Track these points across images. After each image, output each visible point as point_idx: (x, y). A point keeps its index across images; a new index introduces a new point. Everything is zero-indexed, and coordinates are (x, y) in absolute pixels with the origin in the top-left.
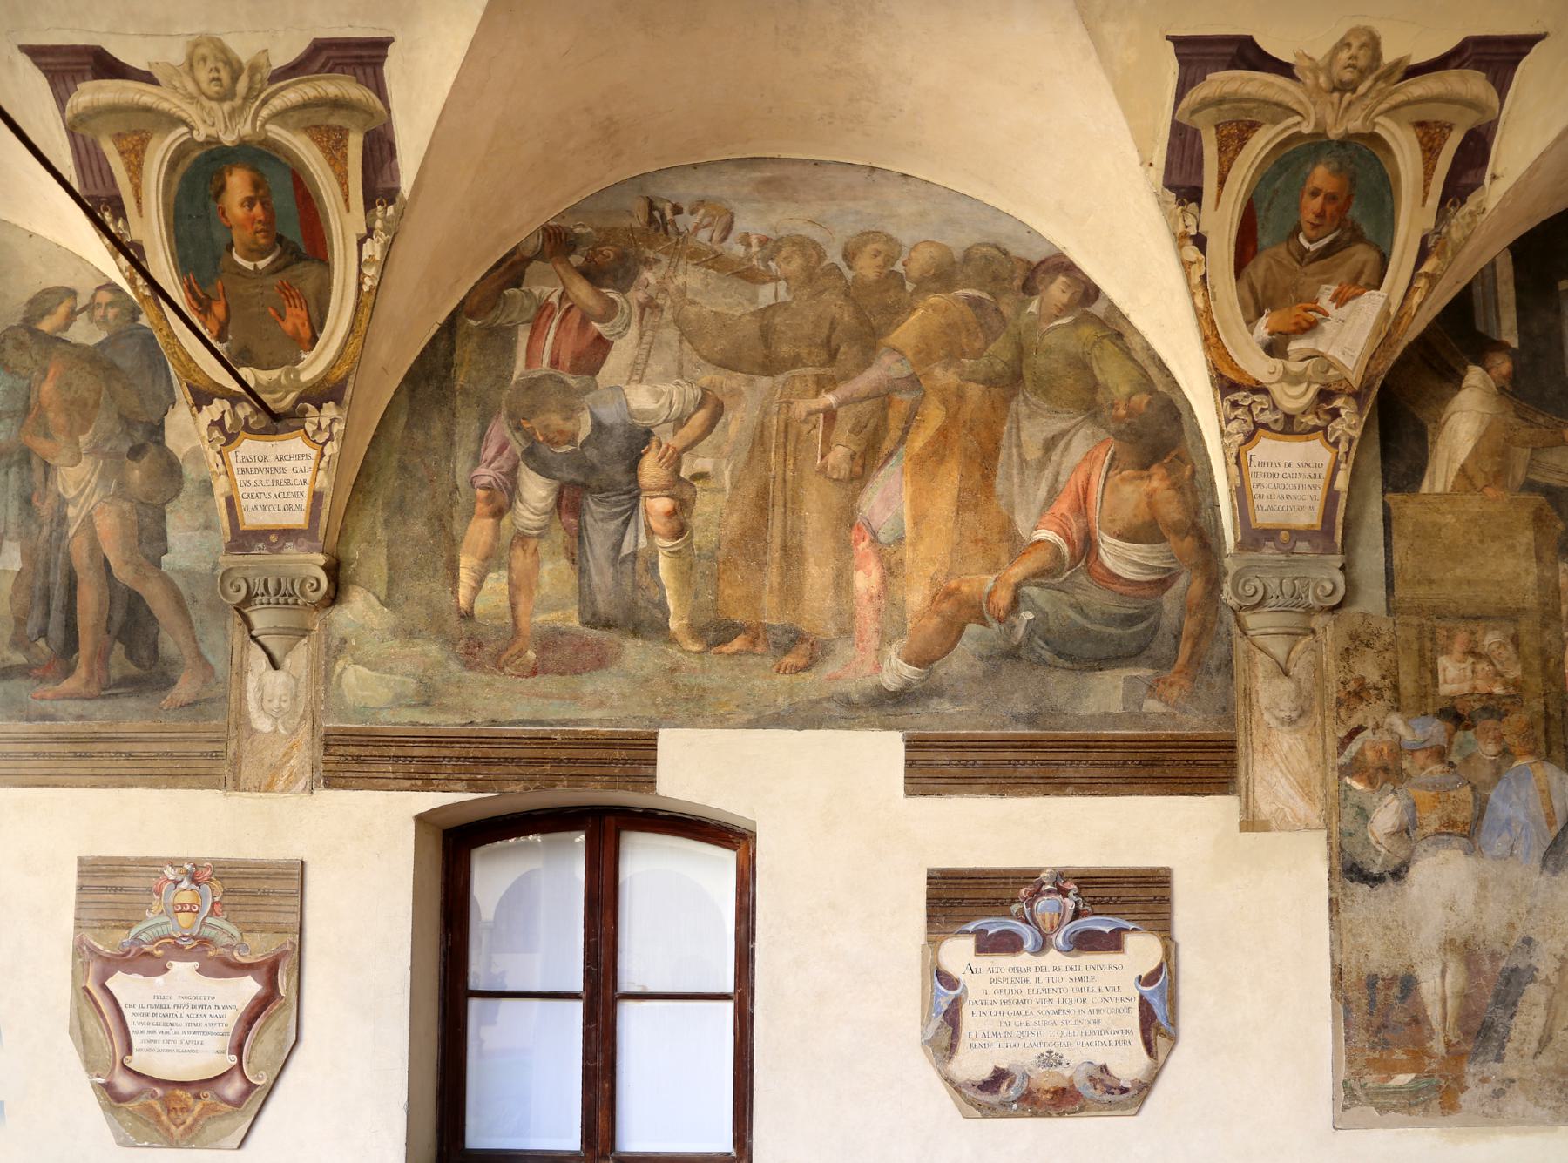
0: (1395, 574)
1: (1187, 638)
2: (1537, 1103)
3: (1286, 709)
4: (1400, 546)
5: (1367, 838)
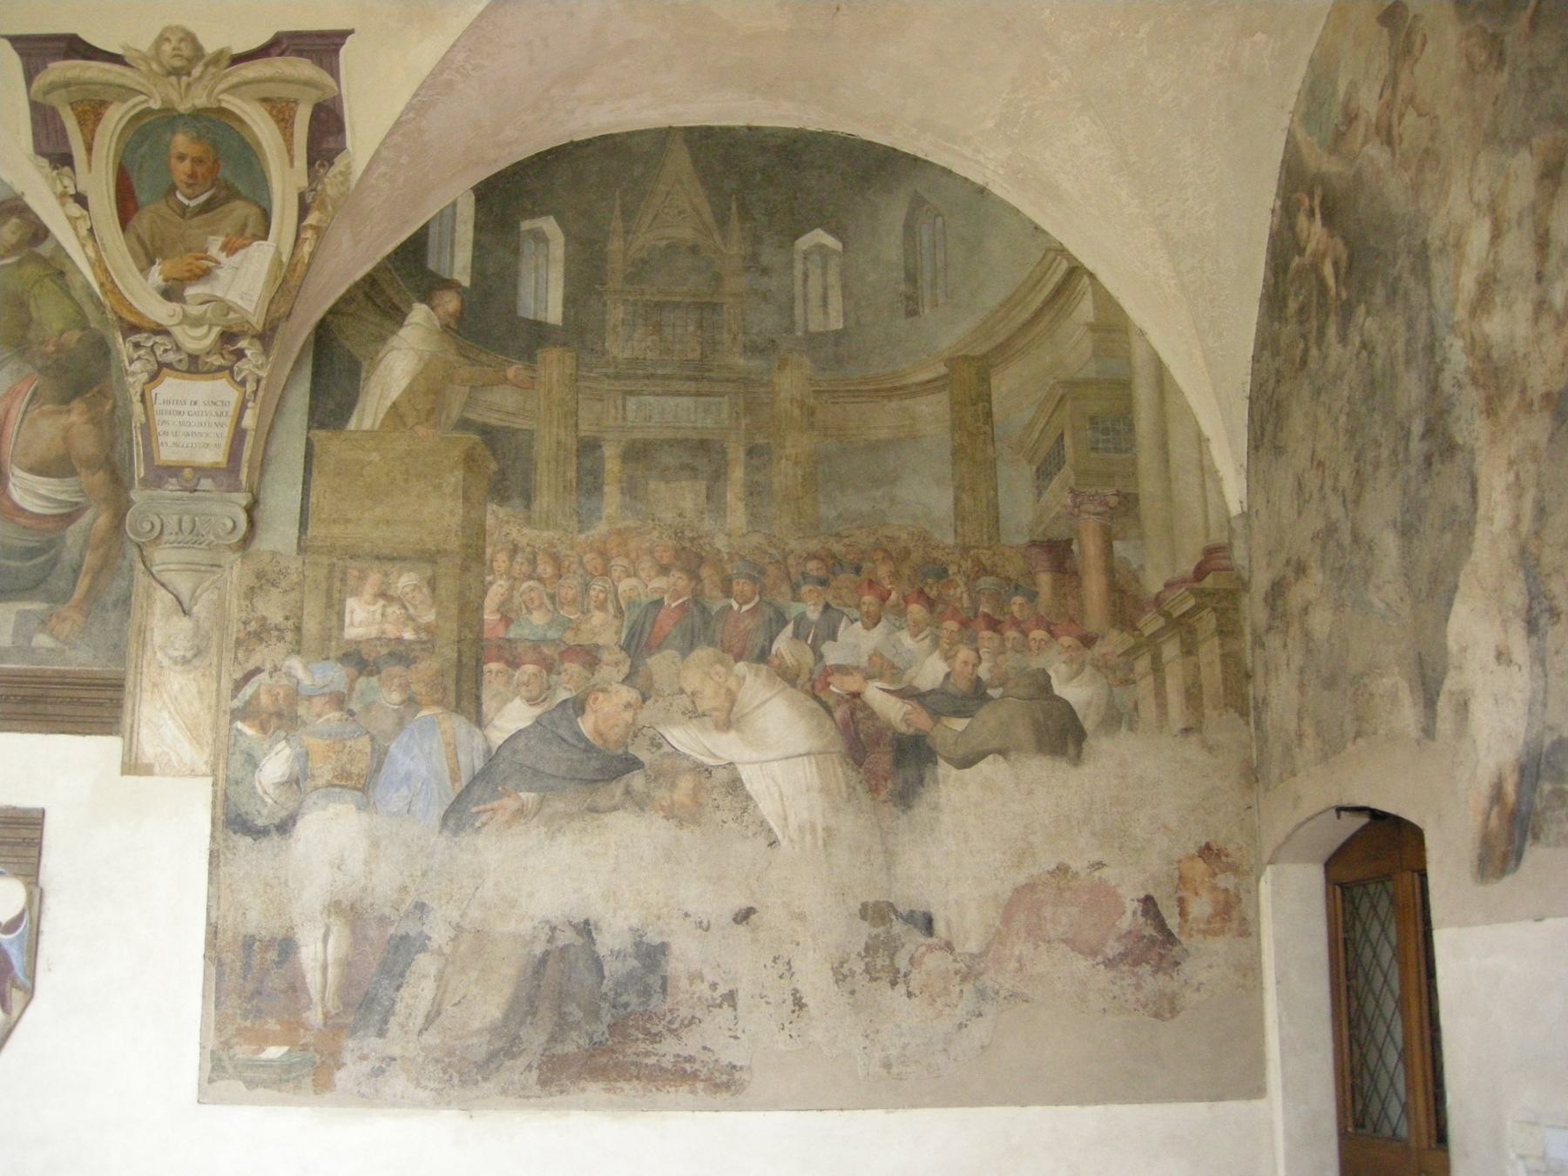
0: (310, 512)
1: (86, 573)
2: (418, 1084)
3: (181, 648)
4: (318, 482)
5: (254, 787)
